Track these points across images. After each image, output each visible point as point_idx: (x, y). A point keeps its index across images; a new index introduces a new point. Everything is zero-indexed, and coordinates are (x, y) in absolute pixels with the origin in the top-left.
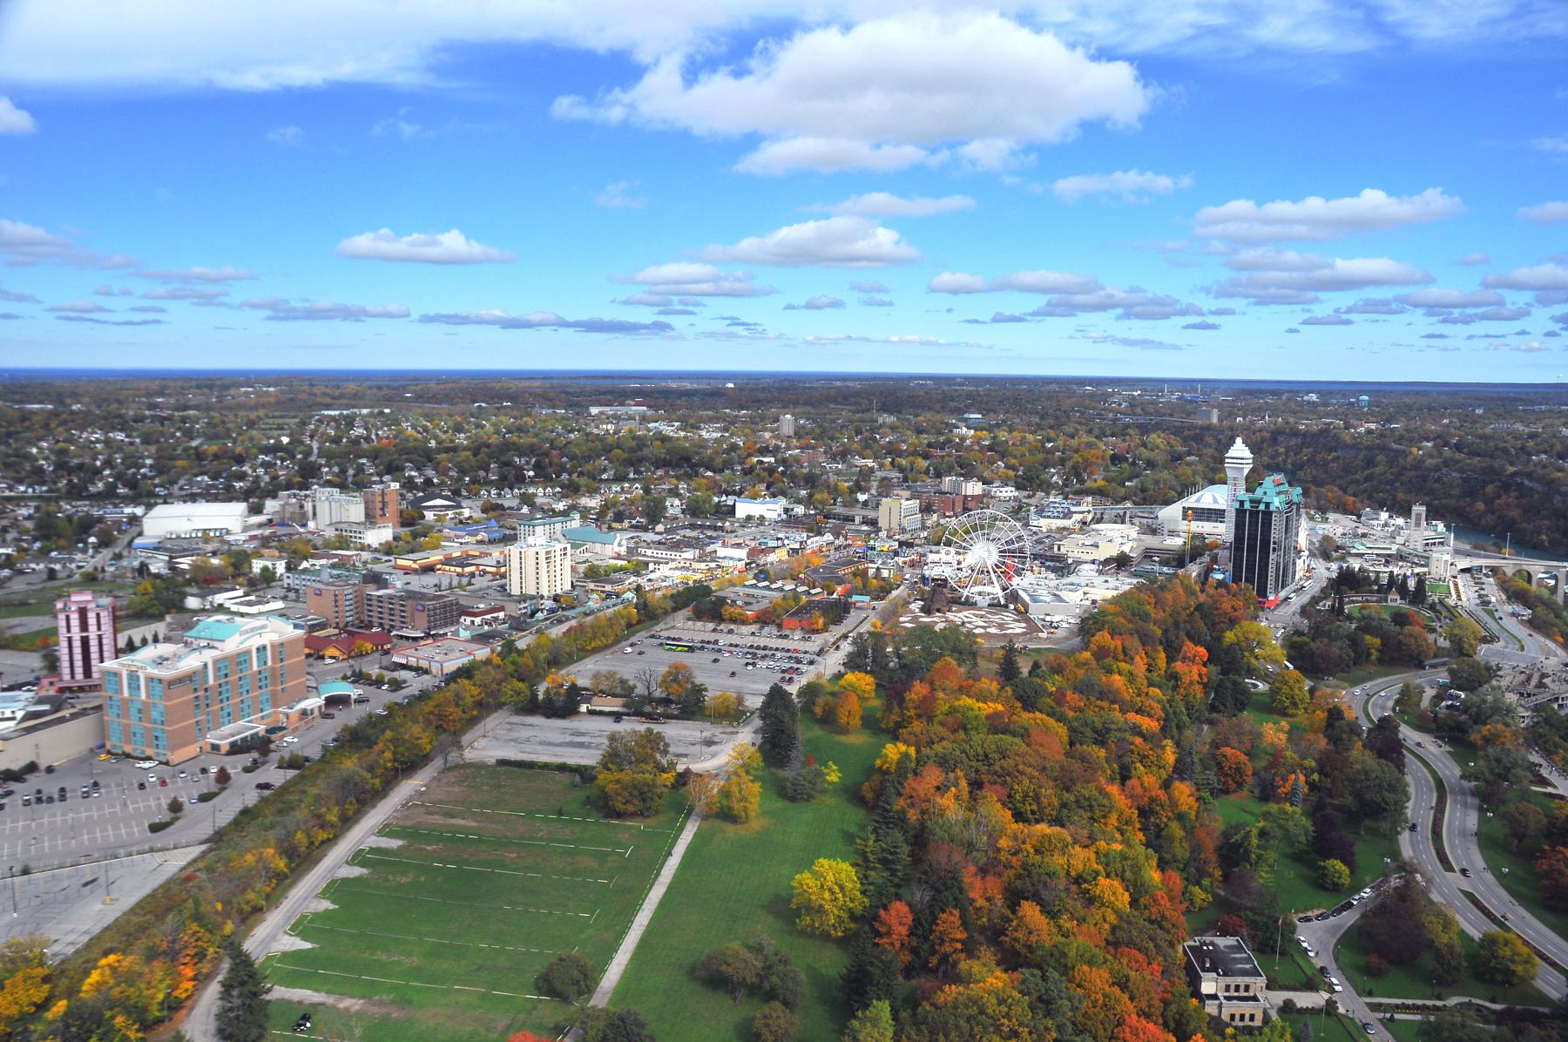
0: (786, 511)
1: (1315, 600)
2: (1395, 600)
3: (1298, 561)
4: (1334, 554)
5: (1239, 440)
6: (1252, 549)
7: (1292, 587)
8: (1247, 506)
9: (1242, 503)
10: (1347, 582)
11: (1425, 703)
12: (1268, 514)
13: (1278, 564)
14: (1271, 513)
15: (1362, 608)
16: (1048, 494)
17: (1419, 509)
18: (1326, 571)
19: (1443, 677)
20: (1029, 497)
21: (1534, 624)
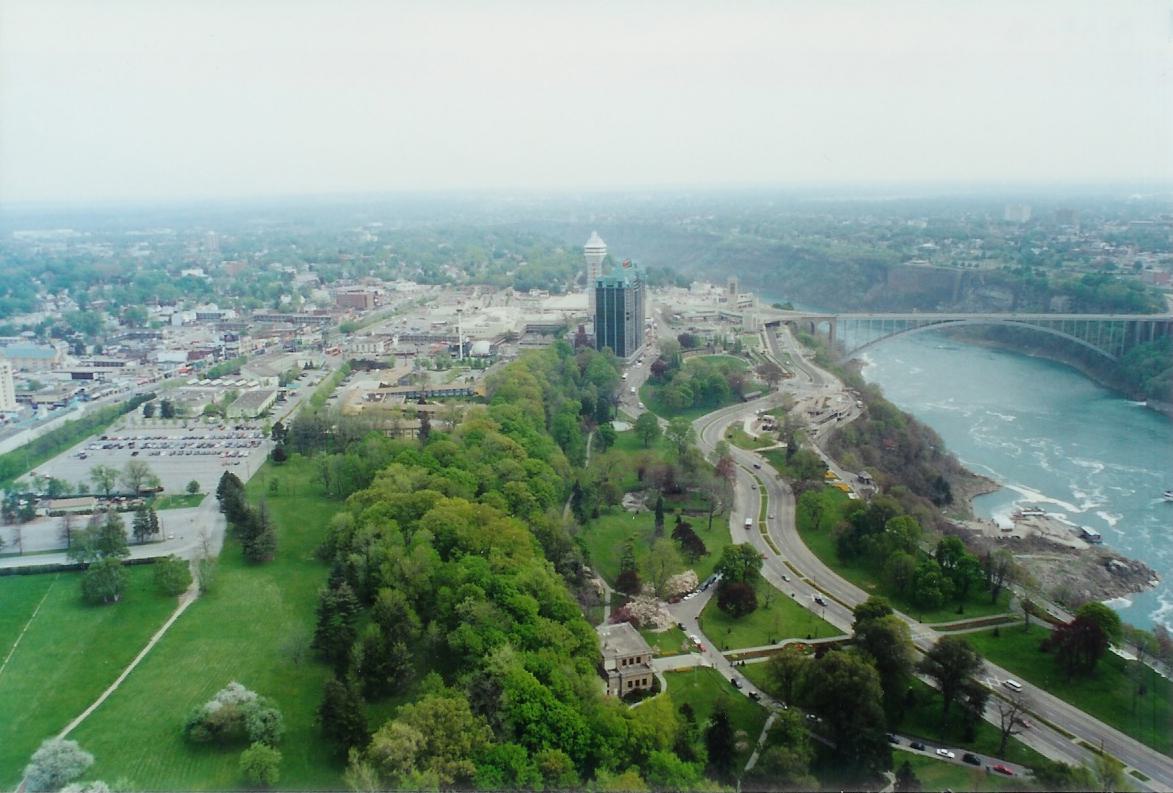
5: (595, 233)
6: (610, 320)
12: (621, 290)
14: (623, 290)
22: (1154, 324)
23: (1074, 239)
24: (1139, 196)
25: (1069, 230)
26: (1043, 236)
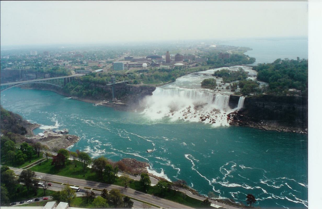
22: (69, 78)
23: (49, 59)
24: (63, 47)
25: (48, 57)
26: (41, 59)
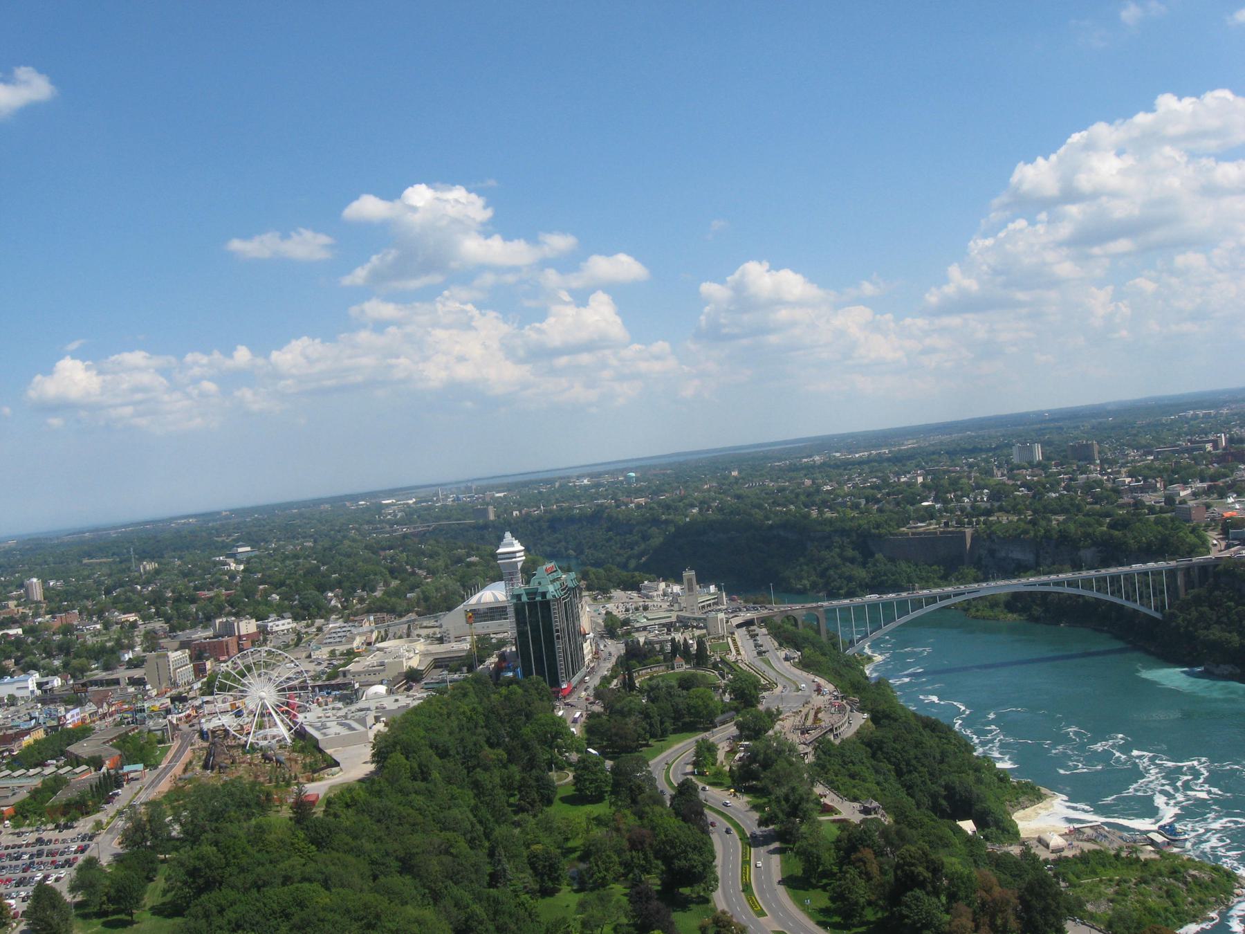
0: (40, 685)
1: (606, 680)
2: (682, 667)
3: (585, 645)
4: (619, 632)
6: (536, 640)
7: (584, 670)
8: (524, 599)
9: (518, 597)
10: (635, 656)
11: (721, 755)
13: (565, 651)
15: (650, 679)
16: (327, 620)
17: (689, 574)
18: (616, 648)
19: (732, 730)
20: (308, 626)
21: (805, 665)
